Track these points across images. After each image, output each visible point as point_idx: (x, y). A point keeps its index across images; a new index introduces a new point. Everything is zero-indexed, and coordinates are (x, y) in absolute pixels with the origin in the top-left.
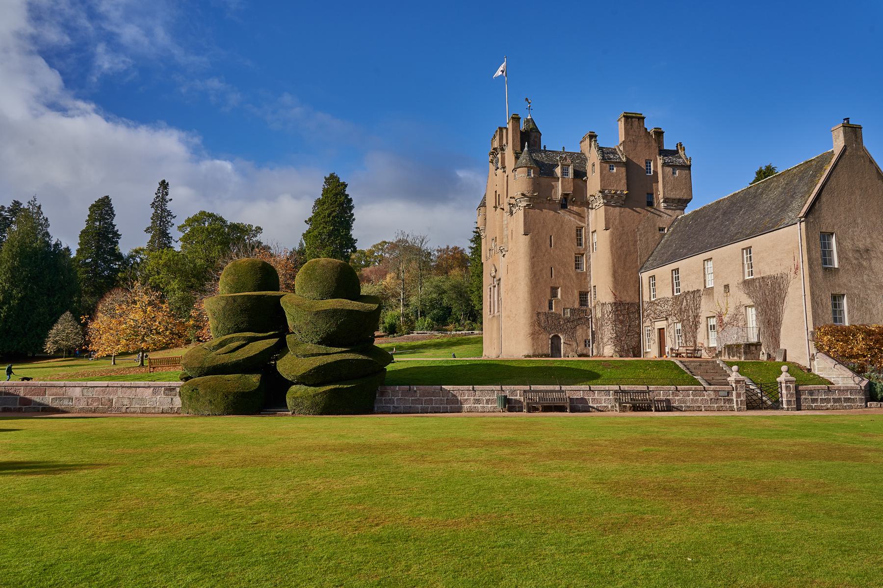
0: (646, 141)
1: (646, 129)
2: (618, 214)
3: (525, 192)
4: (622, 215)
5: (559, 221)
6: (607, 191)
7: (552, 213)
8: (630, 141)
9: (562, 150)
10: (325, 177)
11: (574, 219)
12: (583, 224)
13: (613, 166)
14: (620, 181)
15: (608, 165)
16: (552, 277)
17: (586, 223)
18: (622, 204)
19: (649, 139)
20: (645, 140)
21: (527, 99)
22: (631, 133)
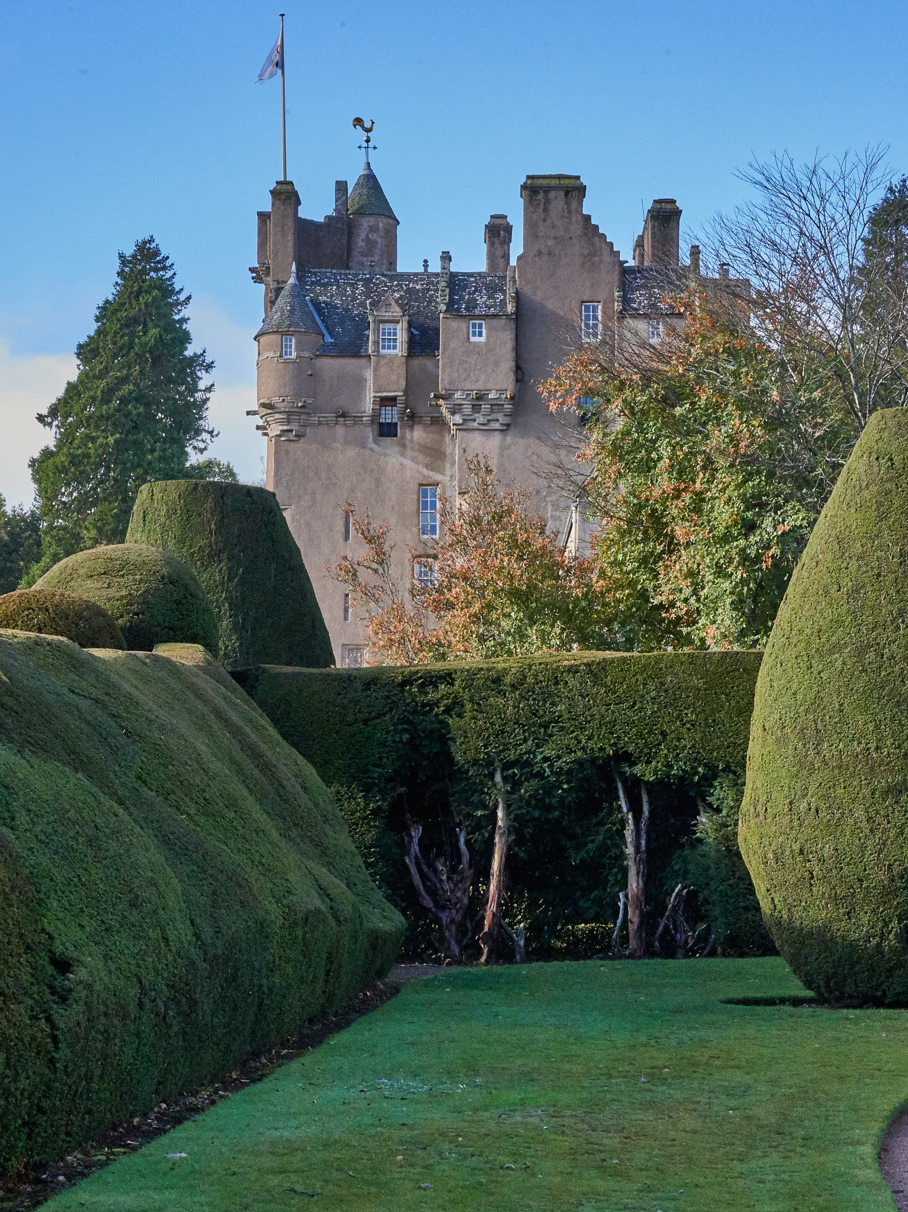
0: (586, 252)
1: (588, 218)
2: (497, 450)
3: (275, 400)
4: (506, 453)
5: (372, 471)
6: (459, 393)
7: (352, 452)
8: (540, 253)
9: (422, 270)
10: (121, 256)
11: (413, 465)
12: (438, 477)
13: (480, 326)
14: (496, 363)
15: (463, 325)
16: (346, 618)
17: (448, 473)
18: (508, 425)
19: (593, 245)
20: (581, 247)
21: (358, 121)
22: (542, 230)
